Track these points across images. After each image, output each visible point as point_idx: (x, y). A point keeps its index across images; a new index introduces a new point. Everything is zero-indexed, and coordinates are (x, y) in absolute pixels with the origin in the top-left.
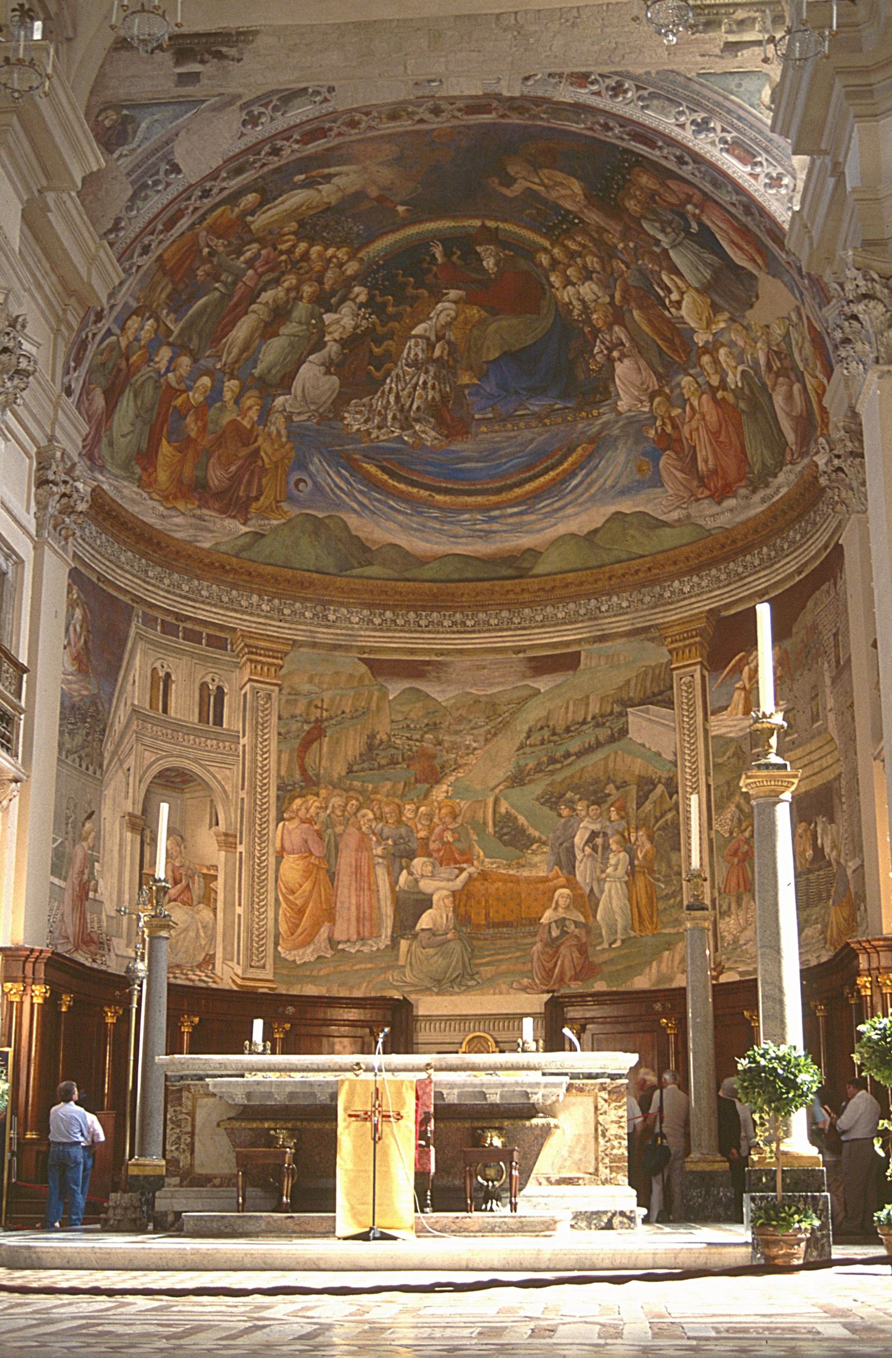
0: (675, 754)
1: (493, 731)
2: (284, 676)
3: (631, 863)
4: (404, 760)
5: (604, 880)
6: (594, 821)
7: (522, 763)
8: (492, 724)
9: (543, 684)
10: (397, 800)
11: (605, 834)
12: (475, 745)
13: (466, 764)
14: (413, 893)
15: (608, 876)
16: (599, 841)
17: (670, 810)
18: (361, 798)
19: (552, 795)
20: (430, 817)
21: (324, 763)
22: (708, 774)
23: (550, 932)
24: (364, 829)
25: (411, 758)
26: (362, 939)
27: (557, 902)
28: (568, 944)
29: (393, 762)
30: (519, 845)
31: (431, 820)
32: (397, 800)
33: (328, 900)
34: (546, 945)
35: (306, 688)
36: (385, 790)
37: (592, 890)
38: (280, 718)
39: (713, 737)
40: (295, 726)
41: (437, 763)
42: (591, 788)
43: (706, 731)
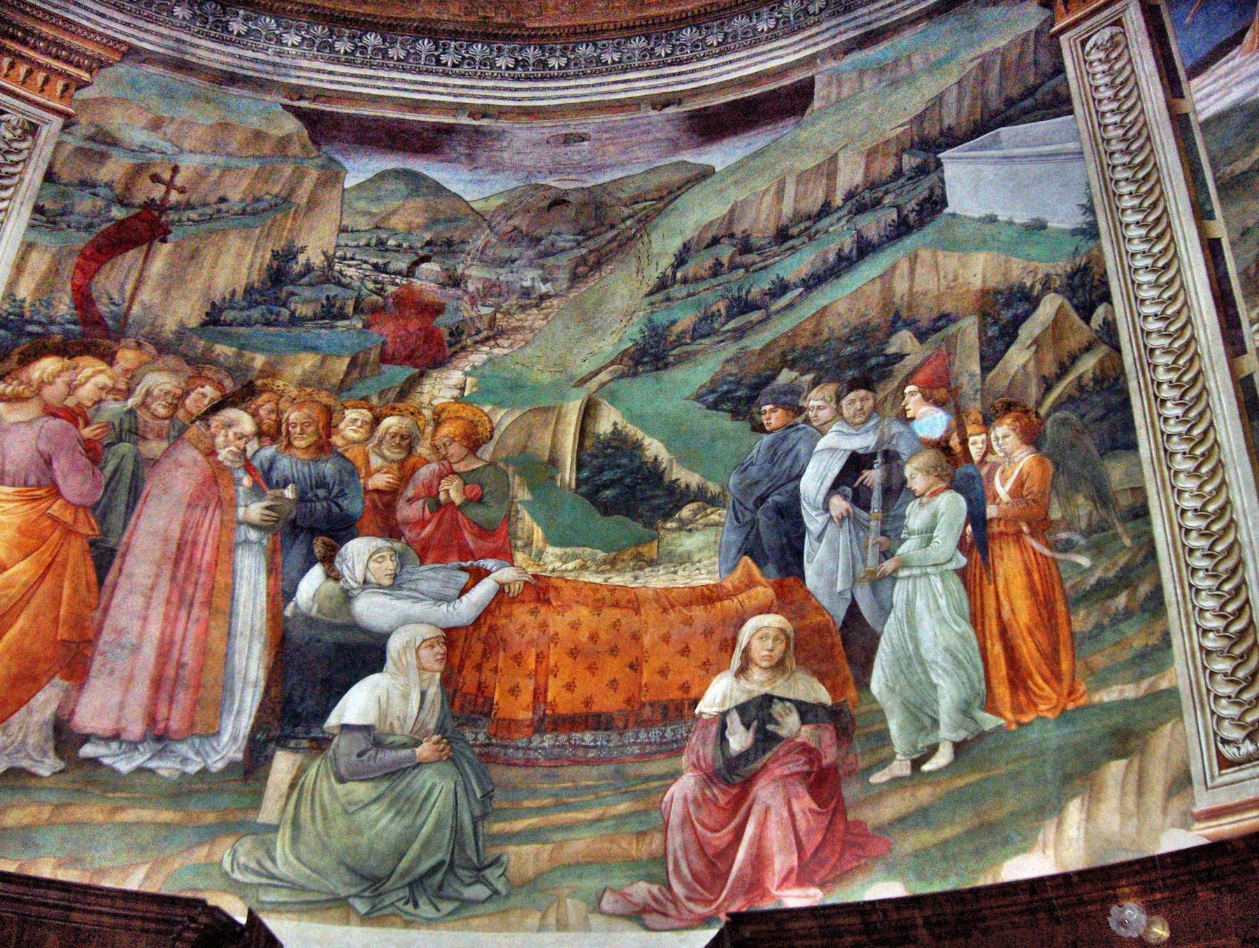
0: (1090, 209)
1: (592, 259)
2: (85, 102)
3: (976, 517)
4: (357, 309)
5: (893, 578)
6: (856, 426)
7: (661, 318)
8: (591, 244)
9: (720, 156)
10: (330, 401)
11: (890, 457)
12: (544, 288)
13: (516, 330)
14: (337, 627)
15: (904, 565)
16: (874, 476)
17: (1088, 348)
18: (228, 383)
19: (739, 383)
20: (408, 442)
21: (145, 295)
22: (1202, 213)
23: (723, 740)
24: (223, 455)
25: (376, 310)
26: (160, 737)
27: (746, 651)
28: (777, 772)
29: (330, 313)
30: (642, 509)
31: (410, 450)
32: (324, 398)
33: (78, 622)
34: (710, 777)
35: (137, 135)
36: (298, 371)
37: (853, 610)
38: (49, 177)
39: (1205, 125)
40: (85, 204)
41: (442, 323)
42: (848, 350)
43: (1180, 123)
